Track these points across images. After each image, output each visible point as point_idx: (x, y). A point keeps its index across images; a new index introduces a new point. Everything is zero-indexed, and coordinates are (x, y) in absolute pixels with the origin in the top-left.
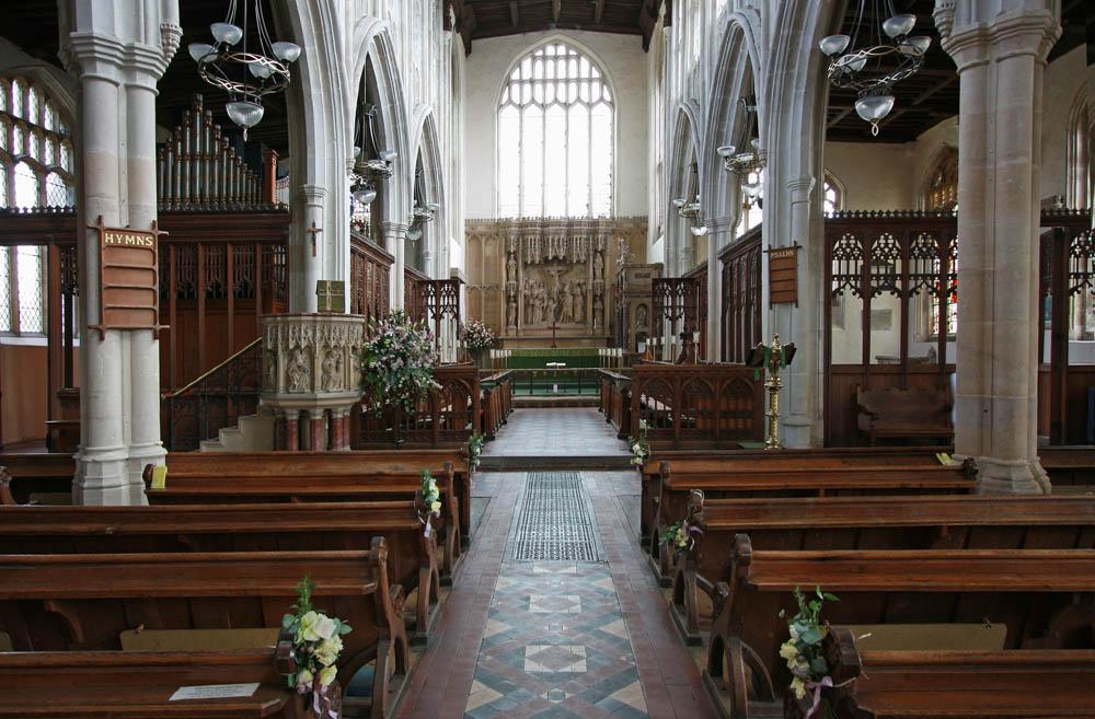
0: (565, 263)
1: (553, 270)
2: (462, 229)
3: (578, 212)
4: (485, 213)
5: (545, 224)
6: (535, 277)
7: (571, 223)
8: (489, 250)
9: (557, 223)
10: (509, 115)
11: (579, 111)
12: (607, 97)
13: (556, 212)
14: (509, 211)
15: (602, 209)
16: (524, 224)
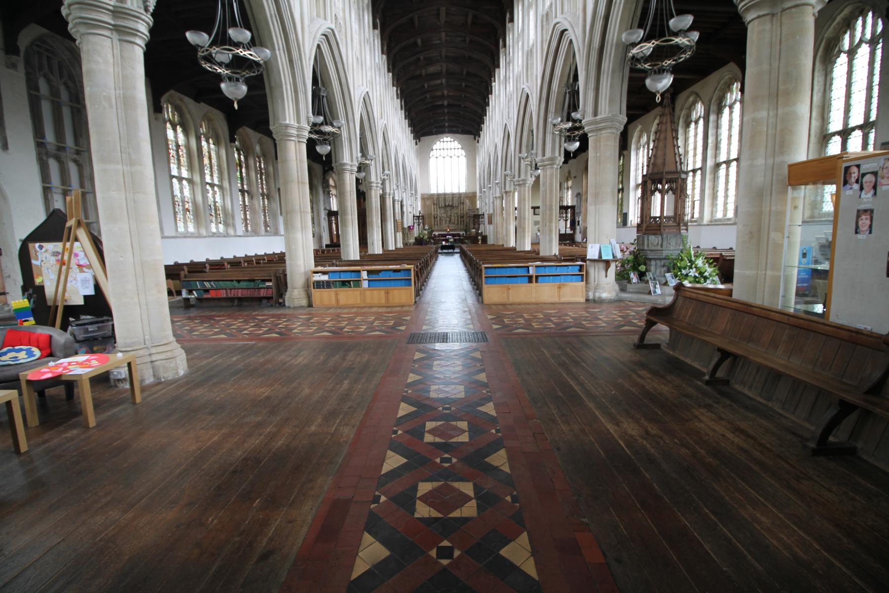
0: (452, 206)
1: (448, 209)
2: (419, 197)
3: (455, 191)
4: (426, 192)
5: (445, 194)
6: (443, 211)
7: (453, 194)
8: (428, 203)
9: (449, 194)
10: (432, 161)
11: (455, 158)
12: (464, 154)
13: (448, 191)
14: (433, 191)
15: (463, 190)
16: (438, 195)
